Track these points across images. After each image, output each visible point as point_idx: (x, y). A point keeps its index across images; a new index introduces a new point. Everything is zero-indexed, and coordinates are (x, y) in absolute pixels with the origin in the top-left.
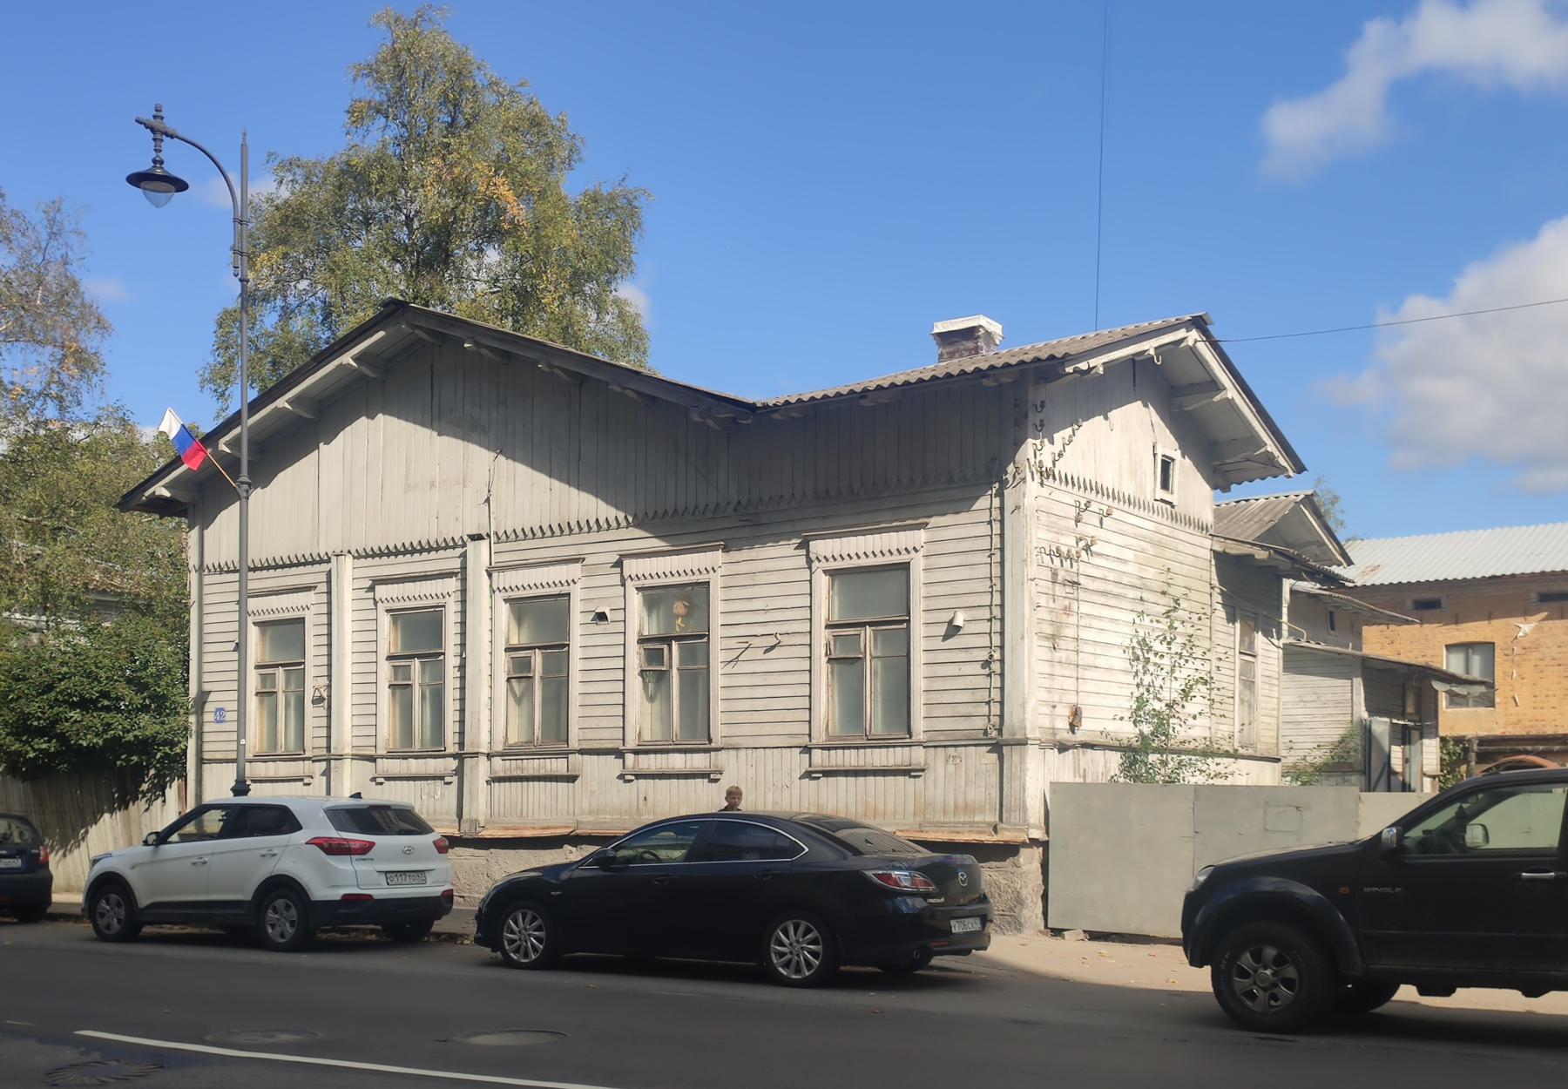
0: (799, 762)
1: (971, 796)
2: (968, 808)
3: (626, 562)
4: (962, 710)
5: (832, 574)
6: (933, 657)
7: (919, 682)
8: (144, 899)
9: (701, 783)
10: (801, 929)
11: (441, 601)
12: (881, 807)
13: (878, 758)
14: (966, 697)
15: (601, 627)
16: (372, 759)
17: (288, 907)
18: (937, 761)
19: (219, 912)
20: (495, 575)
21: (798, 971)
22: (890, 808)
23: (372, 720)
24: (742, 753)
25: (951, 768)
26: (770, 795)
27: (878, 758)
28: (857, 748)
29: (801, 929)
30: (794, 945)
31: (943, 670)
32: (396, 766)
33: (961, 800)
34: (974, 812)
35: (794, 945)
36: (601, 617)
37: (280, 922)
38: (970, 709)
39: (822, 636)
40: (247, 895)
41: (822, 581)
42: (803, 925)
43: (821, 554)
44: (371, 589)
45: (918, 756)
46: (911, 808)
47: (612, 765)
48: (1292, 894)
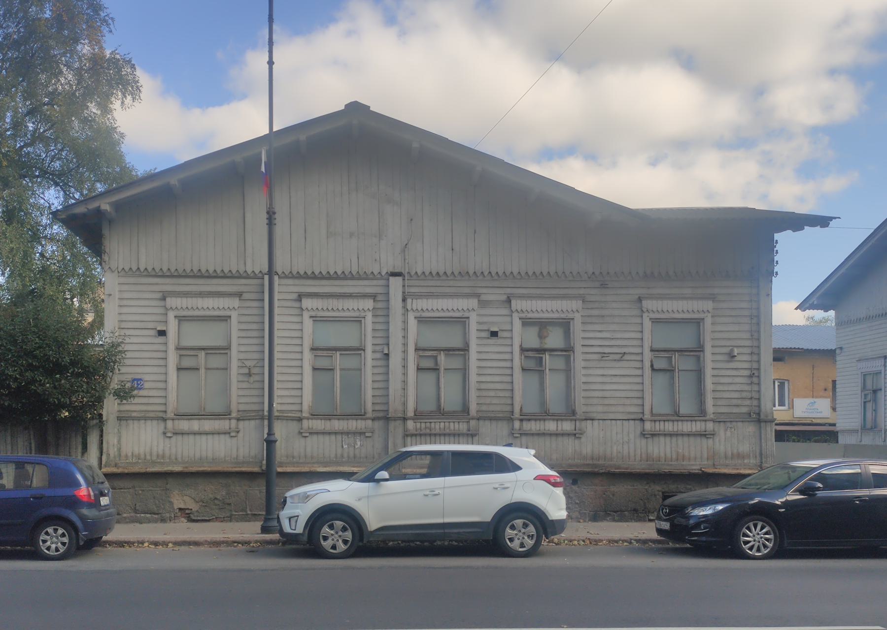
0: (633, 428)
1: (741, 449)
2: (740, 456)
3: (513, 302)
4: (735, 402)
5: (655, 321)
6: (716, 372)
7: (709, 384)
8: (373, 523)
9: (571, 439)
10: (759, 527)
11: (466, 315)
12: (687, 454)
13: (686, 427)
14: (736, 395)
15: (493, 341)
16: (300, 420)
17: (525, 526)
18: (721, 430)
19: (402, 532)
20: (409, 301)
21: (759, 550)
22: (692, 455)
23: (298, 393)
24: (596, 423)
25: (728, 433)
26: (615, 448)
27: (686, 427)
28: (536, 420)
29: (759, 527)
30: (756, 536)
31: (723, 380)
32: (318, 424)
33: (735, 451)
34: (743, 458)
35: (756, 536)
36: (494, 334)
37: (334, 537)
38: (739, 402)
39: (648, 355)
40: (488, 518)
41: (647, 324)
42: (751, 525)
43: (650, 308)
44: (164, 299)
45: (710, 426)
46: (705, 455)
47: (294, 426)
48: (850, 500)
